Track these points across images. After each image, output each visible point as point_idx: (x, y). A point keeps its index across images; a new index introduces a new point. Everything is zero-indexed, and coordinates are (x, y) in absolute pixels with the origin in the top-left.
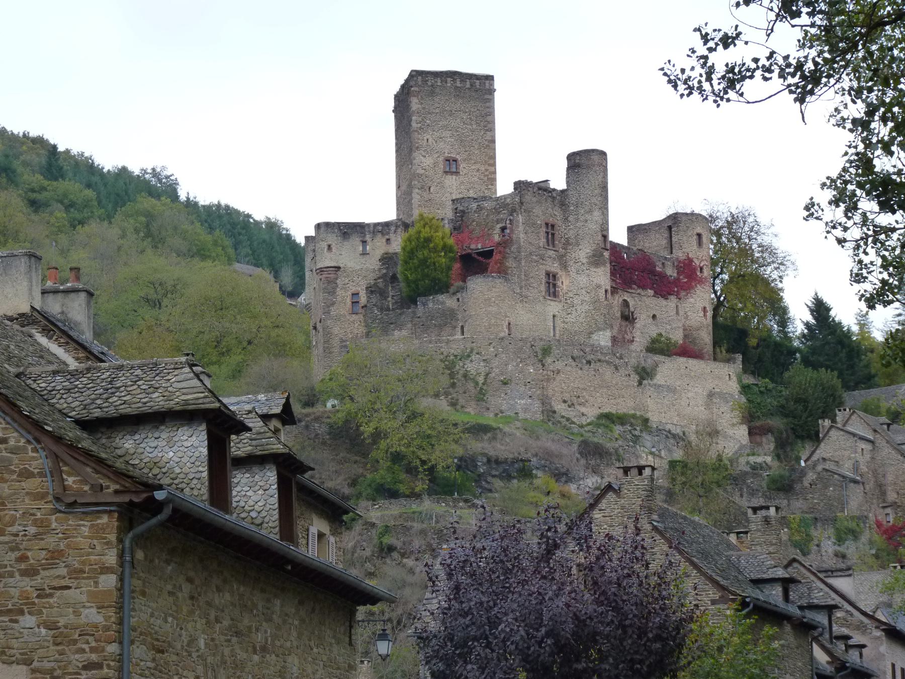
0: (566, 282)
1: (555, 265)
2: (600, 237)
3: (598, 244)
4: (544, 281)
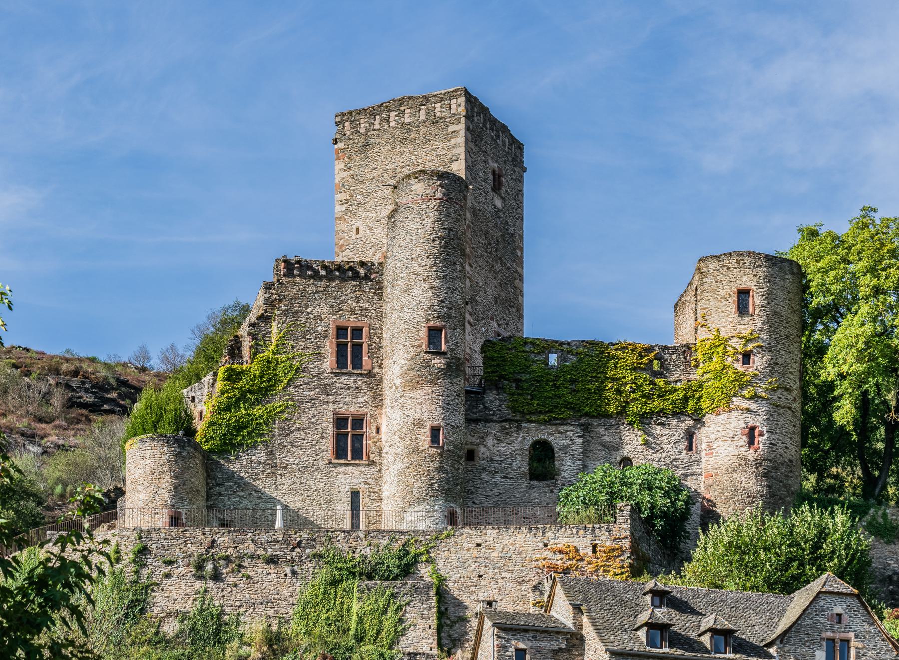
0: (383, 429)
1: (359, 400)
2: (424, 333)
3: (419, 346)
4: (330, 430)
